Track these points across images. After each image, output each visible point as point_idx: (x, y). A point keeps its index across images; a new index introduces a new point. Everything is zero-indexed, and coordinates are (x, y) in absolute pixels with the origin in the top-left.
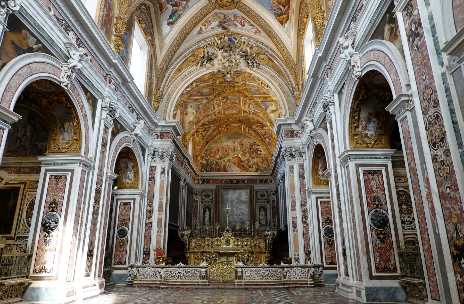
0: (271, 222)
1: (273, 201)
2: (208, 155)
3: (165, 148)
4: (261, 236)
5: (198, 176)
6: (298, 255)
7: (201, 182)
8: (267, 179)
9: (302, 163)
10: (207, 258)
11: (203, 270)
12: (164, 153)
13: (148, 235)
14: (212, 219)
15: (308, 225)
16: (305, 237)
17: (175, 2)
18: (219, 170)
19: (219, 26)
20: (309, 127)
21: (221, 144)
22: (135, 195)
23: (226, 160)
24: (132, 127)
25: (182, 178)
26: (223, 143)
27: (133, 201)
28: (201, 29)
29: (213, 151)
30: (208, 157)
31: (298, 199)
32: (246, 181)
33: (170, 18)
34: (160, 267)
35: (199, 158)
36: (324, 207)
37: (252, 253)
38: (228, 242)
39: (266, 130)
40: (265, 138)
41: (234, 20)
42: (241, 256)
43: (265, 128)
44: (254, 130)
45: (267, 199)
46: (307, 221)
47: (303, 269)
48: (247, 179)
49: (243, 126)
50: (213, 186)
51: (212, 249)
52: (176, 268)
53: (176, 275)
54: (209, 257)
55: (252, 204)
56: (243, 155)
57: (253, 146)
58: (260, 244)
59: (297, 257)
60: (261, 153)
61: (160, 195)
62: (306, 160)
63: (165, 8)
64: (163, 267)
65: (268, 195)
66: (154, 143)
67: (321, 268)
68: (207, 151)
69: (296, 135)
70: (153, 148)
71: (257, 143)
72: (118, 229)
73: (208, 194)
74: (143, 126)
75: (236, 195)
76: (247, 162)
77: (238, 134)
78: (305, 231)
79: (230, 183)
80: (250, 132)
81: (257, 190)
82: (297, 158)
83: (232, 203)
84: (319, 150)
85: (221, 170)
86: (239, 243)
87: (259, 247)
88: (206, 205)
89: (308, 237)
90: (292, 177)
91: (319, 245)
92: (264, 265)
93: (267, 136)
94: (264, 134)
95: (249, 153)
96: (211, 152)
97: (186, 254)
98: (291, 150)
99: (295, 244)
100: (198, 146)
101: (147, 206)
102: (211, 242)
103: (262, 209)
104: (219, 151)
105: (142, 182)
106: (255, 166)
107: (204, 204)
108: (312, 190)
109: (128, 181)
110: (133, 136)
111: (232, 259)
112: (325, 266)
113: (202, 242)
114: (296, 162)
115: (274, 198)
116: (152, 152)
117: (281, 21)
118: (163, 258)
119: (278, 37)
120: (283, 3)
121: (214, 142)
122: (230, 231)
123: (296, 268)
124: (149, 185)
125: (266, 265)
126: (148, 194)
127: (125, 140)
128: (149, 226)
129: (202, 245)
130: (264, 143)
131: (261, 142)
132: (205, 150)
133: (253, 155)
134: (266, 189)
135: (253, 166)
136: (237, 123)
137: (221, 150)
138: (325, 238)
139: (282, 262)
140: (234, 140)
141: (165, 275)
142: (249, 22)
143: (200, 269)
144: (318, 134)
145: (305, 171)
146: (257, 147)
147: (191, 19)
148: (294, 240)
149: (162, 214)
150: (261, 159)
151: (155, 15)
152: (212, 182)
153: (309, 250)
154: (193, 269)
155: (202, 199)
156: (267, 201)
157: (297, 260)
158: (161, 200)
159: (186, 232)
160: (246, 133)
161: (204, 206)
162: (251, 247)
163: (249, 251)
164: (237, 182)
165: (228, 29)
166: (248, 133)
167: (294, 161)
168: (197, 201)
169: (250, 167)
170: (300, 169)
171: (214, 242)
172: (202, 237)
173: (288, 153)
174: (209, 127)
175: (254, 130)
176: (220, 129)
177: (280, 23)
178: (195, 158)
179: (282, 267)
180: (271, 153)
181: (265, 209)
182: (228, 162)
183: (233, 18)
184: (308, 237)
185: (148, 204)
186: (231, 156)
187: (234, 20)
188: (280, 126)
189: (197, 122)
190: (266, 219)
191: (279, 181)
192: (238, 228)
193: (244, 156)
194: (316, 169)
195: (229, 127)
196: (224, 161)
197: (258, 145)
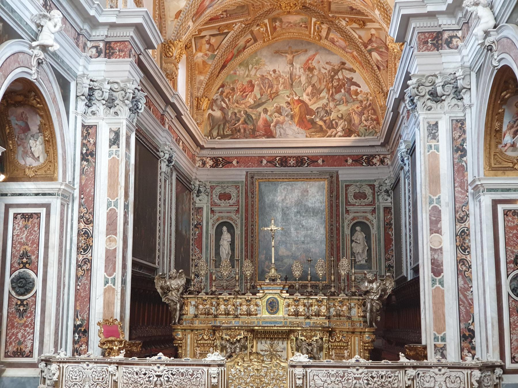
0: (380, 259)
1: (387, 210)
2: (226, 97)
3: (118, 81)
4: (354, 294)
5: (202, 148)
6: (443, 339)
7: (211, 163)
8: (371, 155)
9: (460, 115)
10: (223, 342)
11: (214, 370)
12: (114, 94)
13: (85, 290)
14: (237, 252)
15: (470, 267)
16: (461, 296)
18: (253, 134)
20: (482, 21)
22: (50, 194)
23: (271, 108)
24: (34, 27)
25: (162, 154)
26: (264, 65)
27: (44, 210)
29: (238, 86)
30: (225, 102)
31: (447, 205)
32: (320, 161)
34: (114, 363)
35: (205, 104)
36: (511, 224)
37: (331, 332)
38: (273, 306)
39: (373, 32)
40: (370, 52)
42: (303, 338)
43: (369, 25)
44: (341, 30)
45: (372, 204)
46: (468, 258)
47: (454, 373)
48: (321, 156)
49: (314, 20)
50: (238, 173)
51: (234, 323)
52: (150, 365)
53: (150, 381)
54: (228, 341)
55: (334, 215)
56: (313, 96)
57: (340, 73)
58: (350, 313)
59: (440, 342)
61: (109, 196)
62: (470, 106)
64: (119, 364)
65: (374, 194)
66: (90, 67)
67: (499, 371)
68: (223, 86)
69: (449, 43)
70: (88, 82)
71: (348, 65)
72: (13, 276)
73: (227, 191)
74: (59, 24)
75: (296, 194)
76: (323, 113)
77: (302, 42)
78: (461, 282)
79: (282, 165)
80: (331, 36)
81: (346, 181)
82: (450, 102)
83: (285, 214)
84: (506, 82)
85: (258, 133)
86: (301, 309)
87: (349, 318)
88: (222, 218)
89: (470, 297)
90: (433, 150)
91: (496, 316)
92: (357, 361)
93: (375, 45)
94: (366, 41)
95: (329, 90)
96: (233, 89)
97: (174, 334)
98: (434, 83)
99: (435, 312)
100: (200, 73)
101: (79, 222)
102: (234, 305)
103: (358, 228)
104: (253, 86)
105: (65, 165)
106: (342, 124)
107: (217, 215)
108: (483, 182)
109: (30, 161)
110: (37, 52)
111: (282, 346)
112: (509, 365)
113: (212, 304)
114: (445, 113)
115: (389, 202)
116: (86, 91)
118: (121, 342)
121: (241, 64)
122: (279, 281)
123: (436, 370)
124: (82, 172)
125: (362, 361)
126: (80, 194)
127: (16, 61)
128: (84, 267)
129: (213, 311)
130: (366, 63)
131: (360, 63)
132: (219, 83)
133: (337, 96)
134: (370, 181)
136: (298, 13)
137: (258, 85)
138: (511, 300)
139: (401, 355)
140: (290, 57)
141: (125, 381)
143: (205, 369)
144: (505, 40)
145: (468, 135)
146: (348, 75)
148: (434, 303)
149: (115, 241)
150: (359, 105)
152: (238, 162)
153: (471, 327)
154: (191, 369)
155: (213, 204)
156: (370, 208)
157: (441, 351)
158: (112, 207)
159: (173, 282)
160: (321, 38)
161: (218, 220)
162: (329, 318)
163: (324, 327)
164: (297, 162)
166: (326, 38)
167: (439, 110)
168: (200, 209)
169: (331, 126)
170: (453, 129)
171: (241, 305)
172: (213, 293)
173: (424, 90)
174: (227, 26)
175: (341, 30)
176: (255, 29)
178: (195, 103)
179: (403, 367)
180: (385, 91)
181: (365, 228)
182: (276, 114)
184: (470, 297)
185: (80, 218)
186: (283, 98)
188: (406, 20)
189: (197, 13)
190: (369, 251)
191: (403, 161)
192: (297, 273)
193: (315, 98)
194: (497, 131)
195: (278, 24)
196: (266, 111)
197: (352, 70)
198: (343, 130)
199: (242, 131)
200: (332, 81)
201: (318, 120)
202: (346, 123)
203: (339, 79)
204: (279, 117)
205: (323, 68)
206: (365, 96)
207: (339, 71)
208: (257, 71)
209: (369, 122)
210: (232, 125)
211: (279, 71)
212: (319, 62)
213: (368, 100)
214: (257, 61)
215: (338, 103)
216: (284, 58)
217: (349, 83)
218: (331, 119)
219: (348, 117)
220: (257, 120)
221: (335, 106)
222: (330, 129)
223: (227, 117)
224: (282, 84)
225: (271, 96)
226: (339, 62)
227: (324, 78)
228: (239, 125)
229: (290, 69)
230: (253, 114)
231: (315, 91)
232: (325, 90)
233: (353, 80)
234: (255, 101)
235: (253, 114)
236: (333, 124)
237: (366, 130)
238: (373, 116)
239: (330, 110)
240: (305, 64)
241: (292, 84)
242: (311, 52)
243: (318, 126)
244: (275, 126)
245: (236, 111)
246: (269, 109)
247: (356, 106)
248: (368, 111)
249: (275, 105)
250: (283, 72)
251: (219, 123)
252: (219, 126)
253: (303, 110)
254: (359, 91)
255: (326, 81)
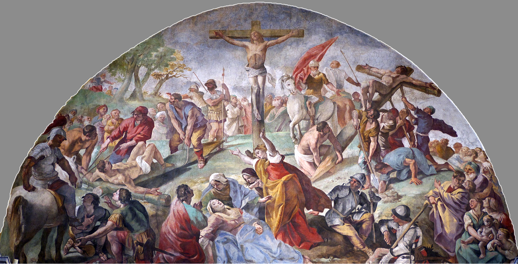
2: (70, 151)
21: (161, 79)
26: (183, 67)
30: (66, 167)
56: (322, 156)
57: (396, 96)
60: (452, 141)
76: (351, 203)
96: (91, 131)
104: (149, 124)
135: (392, 233)
137: (163, 121)
140: (254, 49)
182: (216, 203)
193: (327, 163)
198: (412, 252)
199: (114, 248)
200: (375, 117)
201: (337, 221)
202: (419, 232)
203: (394, 111)
204: (224, 211)
205: (349, 80)
206: (470, 159)
207: (392, 90)
208: (161, 83)
209: (485, 231)
210: (83, 233)
211: (224, 86)
212: (338, 65)
213: (478, 169)
214: (161, 57)
215: (393, 175)
216: (239, 53)
217: (423, 123)
218: (377, 220)
219: (423, 216)
220: (161, 217)
221: (387, 186)
222: (373, 248)
223: (69, 207)
224: (233, 120)
225: (200, 153)
226: (393, 66)
227: (353, 108)
228: (106, 232)
229: (256, 81)
230: (149, 201)
231: (327, 142)
232: (357, 138)
233: (434, 116)
234: (153, 166)
235: (149, 201)
236: (381, 235)
237: (478, 253)
238: (494, 215)
239: (372, 194)
240: (298, 69)
241: (261, 122)
242: (313, 37)
243: (339, 238)
244: (212, 236)
245: (98, 191)
246: (194, 187)
247: (446, 185)
248: (480, 201)
249: (212, 178)
250: (235, 88)
251: (47, 226)
252: (47, 232)
253: (293, 192)
254: (451, 144)
255: (360, 117)
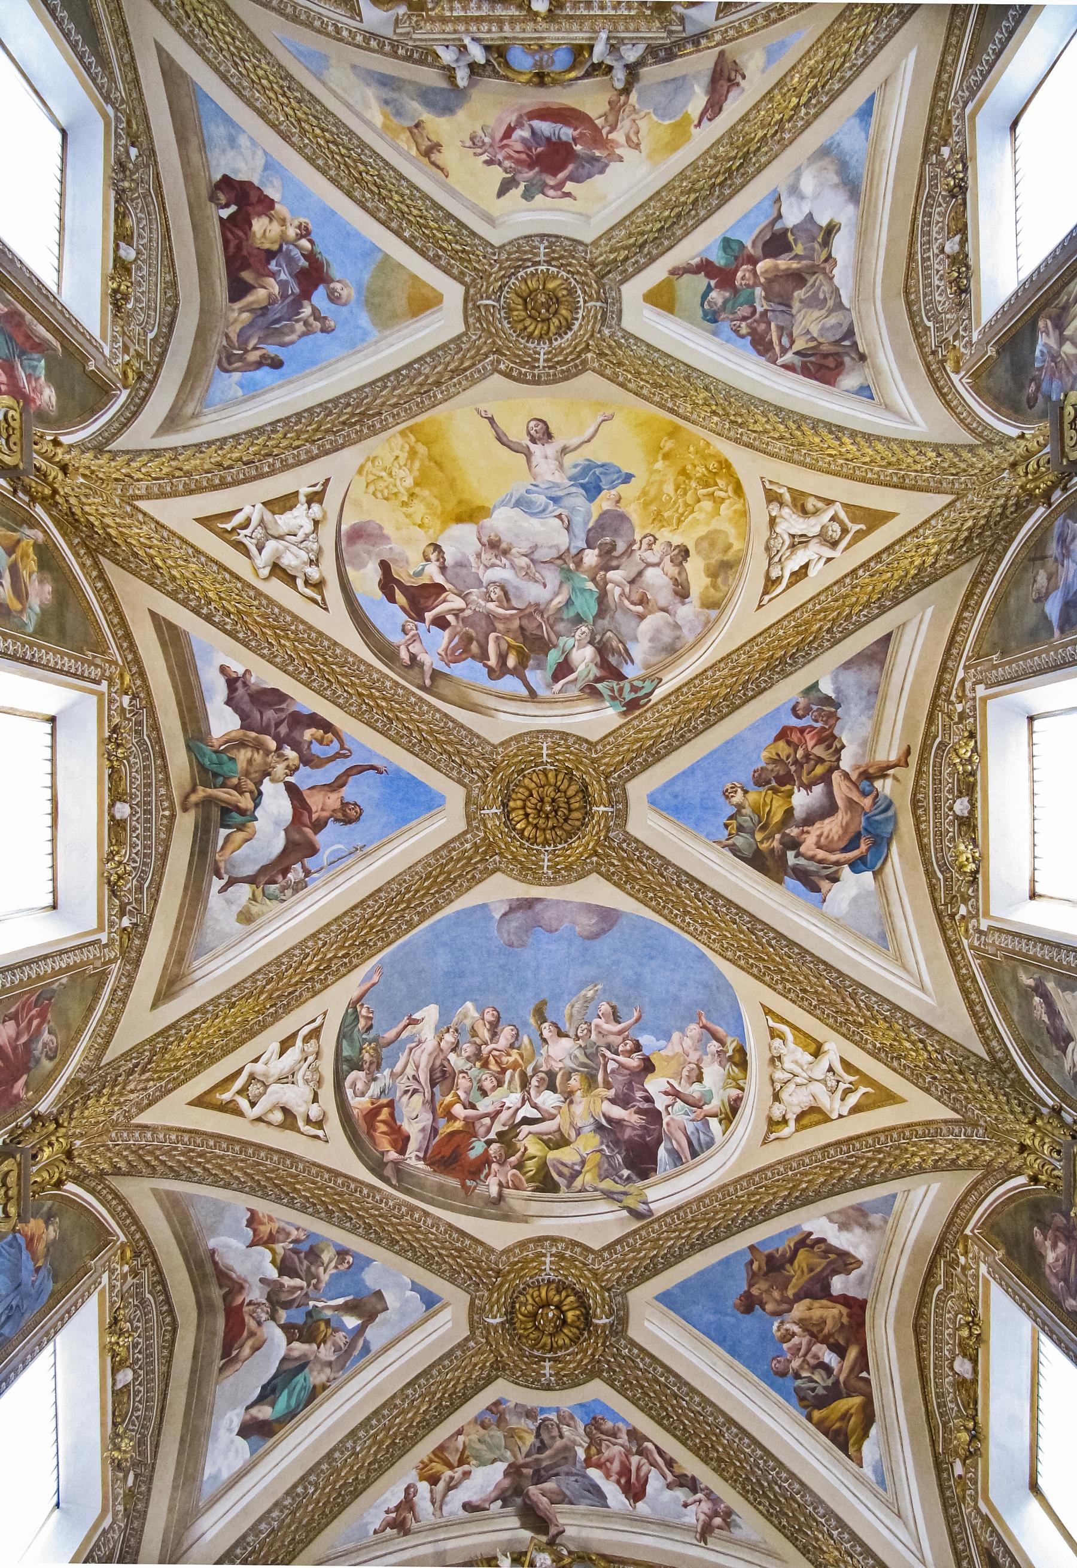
17: (309, 1314)
19: (504, 1497)
28: (408, 1503)
33: (260, 1400)
41: (588, 1462)
63: (250, 1343)
117: (838, 1432)
119: (839, 1519)
120: (831, 1335)
142: (670, 1463)
147: (368, 1419)
151: (193, 1371)
165: (553, 1531)
177: (833, 1440)
183: (585, 1441)
187: (588, 1462)
